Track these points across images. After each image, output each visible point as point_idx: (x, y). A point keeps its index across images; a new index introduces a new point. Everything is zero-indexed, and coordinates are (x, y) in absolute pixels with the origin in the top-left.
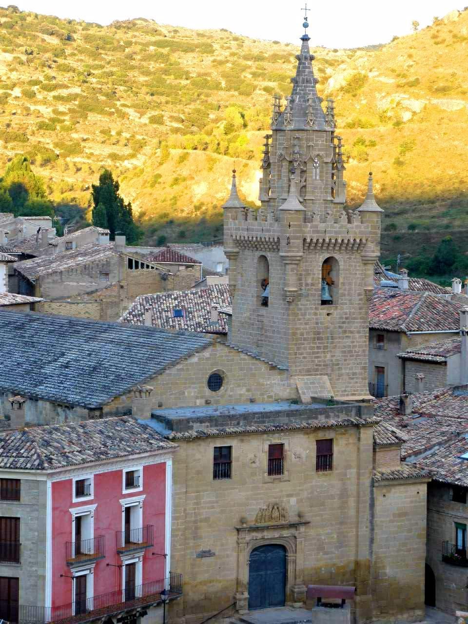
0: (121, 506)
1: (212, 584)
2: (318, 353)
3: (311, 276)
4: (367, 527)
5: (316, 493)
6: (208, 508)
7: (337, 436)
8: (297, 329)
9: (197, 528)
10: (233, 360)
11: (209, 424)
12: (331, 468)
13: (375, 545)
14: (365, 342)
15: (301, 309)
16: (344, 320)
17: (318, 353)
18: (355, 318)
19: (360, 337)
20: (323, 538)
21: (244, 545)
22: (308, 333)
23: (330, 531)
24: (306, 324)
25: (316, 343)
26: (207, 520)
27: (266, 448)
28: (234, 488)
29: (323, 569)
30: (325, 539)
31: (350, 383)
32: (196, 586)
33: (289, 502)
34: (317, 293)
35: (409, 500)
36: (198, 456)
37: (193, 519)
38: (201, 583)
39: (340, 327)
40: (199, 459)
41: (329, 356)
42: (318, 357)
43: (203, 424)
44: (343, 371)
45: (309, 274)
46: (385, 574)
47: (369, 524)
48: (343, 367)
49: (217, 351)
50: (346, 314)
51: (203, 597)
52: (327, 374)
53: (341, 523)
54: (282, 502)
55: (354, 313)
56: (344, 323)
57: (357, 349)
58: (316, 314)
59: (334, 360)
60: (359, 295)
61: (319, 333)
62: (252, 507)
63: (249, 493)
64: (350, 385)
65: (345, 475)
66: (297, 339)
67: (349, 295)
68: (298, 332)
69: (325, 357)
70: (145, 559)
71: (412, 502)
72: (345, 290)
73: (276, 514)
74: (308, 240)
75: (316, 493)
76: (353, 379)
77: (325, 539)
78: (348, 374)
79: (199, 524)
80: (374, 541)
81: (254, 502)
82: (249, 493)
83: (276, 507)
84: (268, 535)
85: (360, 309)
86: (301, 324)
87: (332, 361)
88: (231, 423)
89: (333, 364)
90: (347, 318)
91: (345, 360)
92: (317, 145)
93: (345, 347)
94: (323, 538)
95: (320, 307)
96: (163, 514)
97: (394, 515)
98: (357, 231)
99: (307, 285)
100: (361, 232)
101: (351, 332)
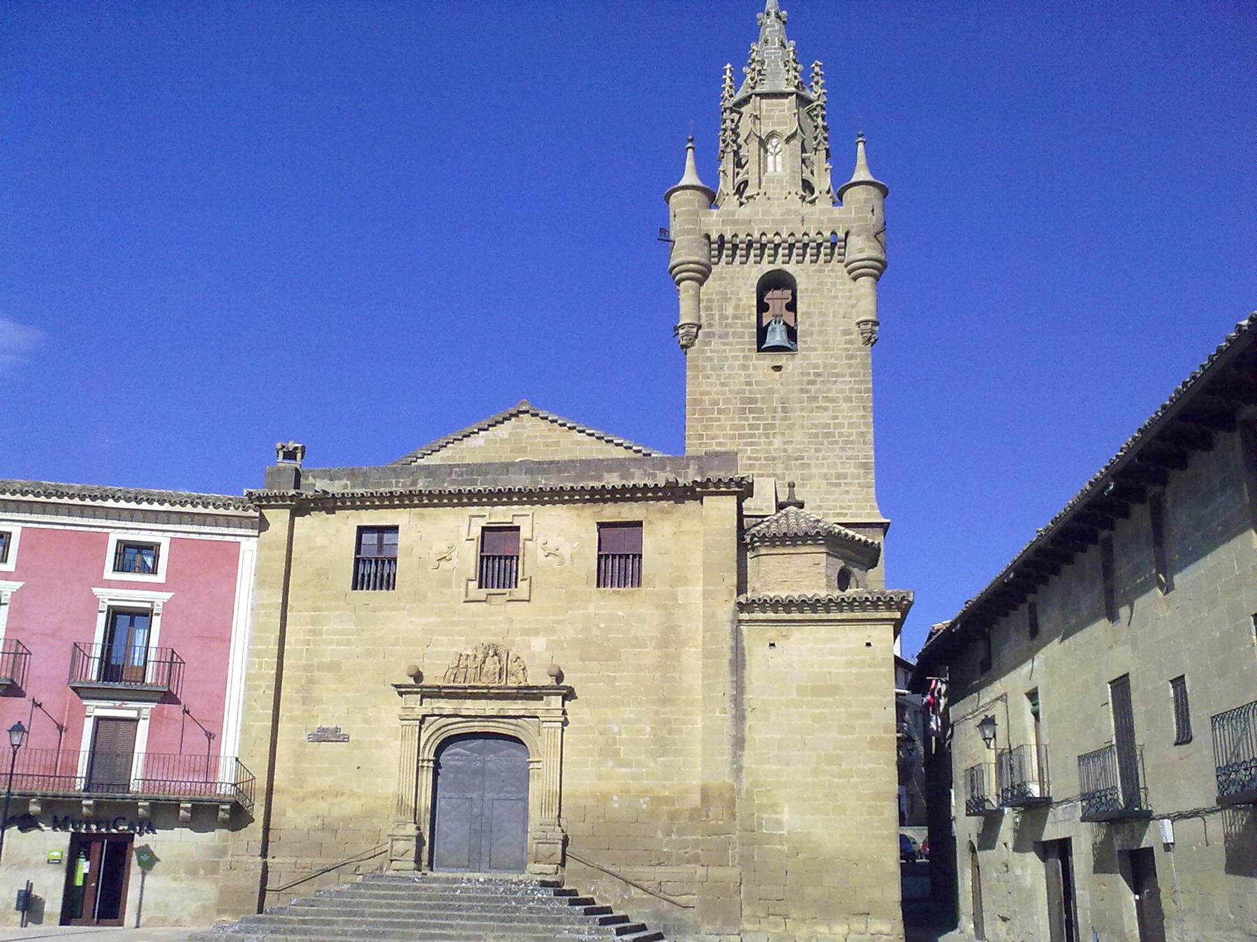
0: (95, 601)
1: (339, 799)
2: (752, 436)
3: (733, 303)
4: (724, 711)
5: (595, 631)
6: (338, 644)
7: (651, 517)
8: (702, 393)
9: (311, 681)
10: (558, 443)
11: (348, 483)
12: (637, 581)
13: (748, 758)
14: (864, 417)
15: (710, 359)
16: (812, 378)
17: (752, 436)
18: (837, 375)
19: (852, 409)
20: (616, 729)
22: (726, 401)
23: (632, 716)
24: (722, 384)
25: (747, 419)
26: (333, 667)
27: (477, 532)
28: (398, 609)
29: (615, 798)
30: (620, 733)
31: (833, 493)
32: (304, 799)
33: (529, 646)
34: (747, 331)
35: (844, 658)
36: (320, 541)
37: (304, 662)
38: (315, 794)
39: (802, 391)
40: (324, 547)
41: (777, 442)
42: (752, 444)
43: (336, 482)
44: (814, 470)
45: (727, 300)
46: (779, 823)
47: (728, 705)
48: (812, 462)
49: (525, 427)
50: (816, 366)
51: (318, 823)
52: (774, 475)
53: (664, 701)
54: (512, 643)
55: (835, 366)
56: (811, 383)
57: (845, 430)
58: (745, 367)
59: (789, 450)
60: (846, 332)
61: (752, 401)
63: (433, 620)
64: (830, 497)
65: (674, 597)
66: (703, 411)
67: (821, 332)
68: (706, 398)
69: (770, 443)
70: (155, 719)
71: (850, 664)
72: (812, 325)
73: (491, 665)
74: (714, 237)
75: (595, 631)
76: (838, 485)
77: (620, 733)
78: (825, 477)
79: (316, 673)
80: (746, 745)
81: (444, 639)
82: (433, 620)
84: (470, 707)
85: (851, 357)
86: (712, 384)
87: (785, 451)
88: (397, 482)
89: (789, 458)
90: (818, 375)
91: (817, 450)
92: (771, 117)
93: (815, 426)
94: (616, 729)
95: (754, 354)
96: (226, 640)
97: (801, 691)
98: (824, 218)
99: (723, 317)
100: (831, 220)
101: (831, 400)
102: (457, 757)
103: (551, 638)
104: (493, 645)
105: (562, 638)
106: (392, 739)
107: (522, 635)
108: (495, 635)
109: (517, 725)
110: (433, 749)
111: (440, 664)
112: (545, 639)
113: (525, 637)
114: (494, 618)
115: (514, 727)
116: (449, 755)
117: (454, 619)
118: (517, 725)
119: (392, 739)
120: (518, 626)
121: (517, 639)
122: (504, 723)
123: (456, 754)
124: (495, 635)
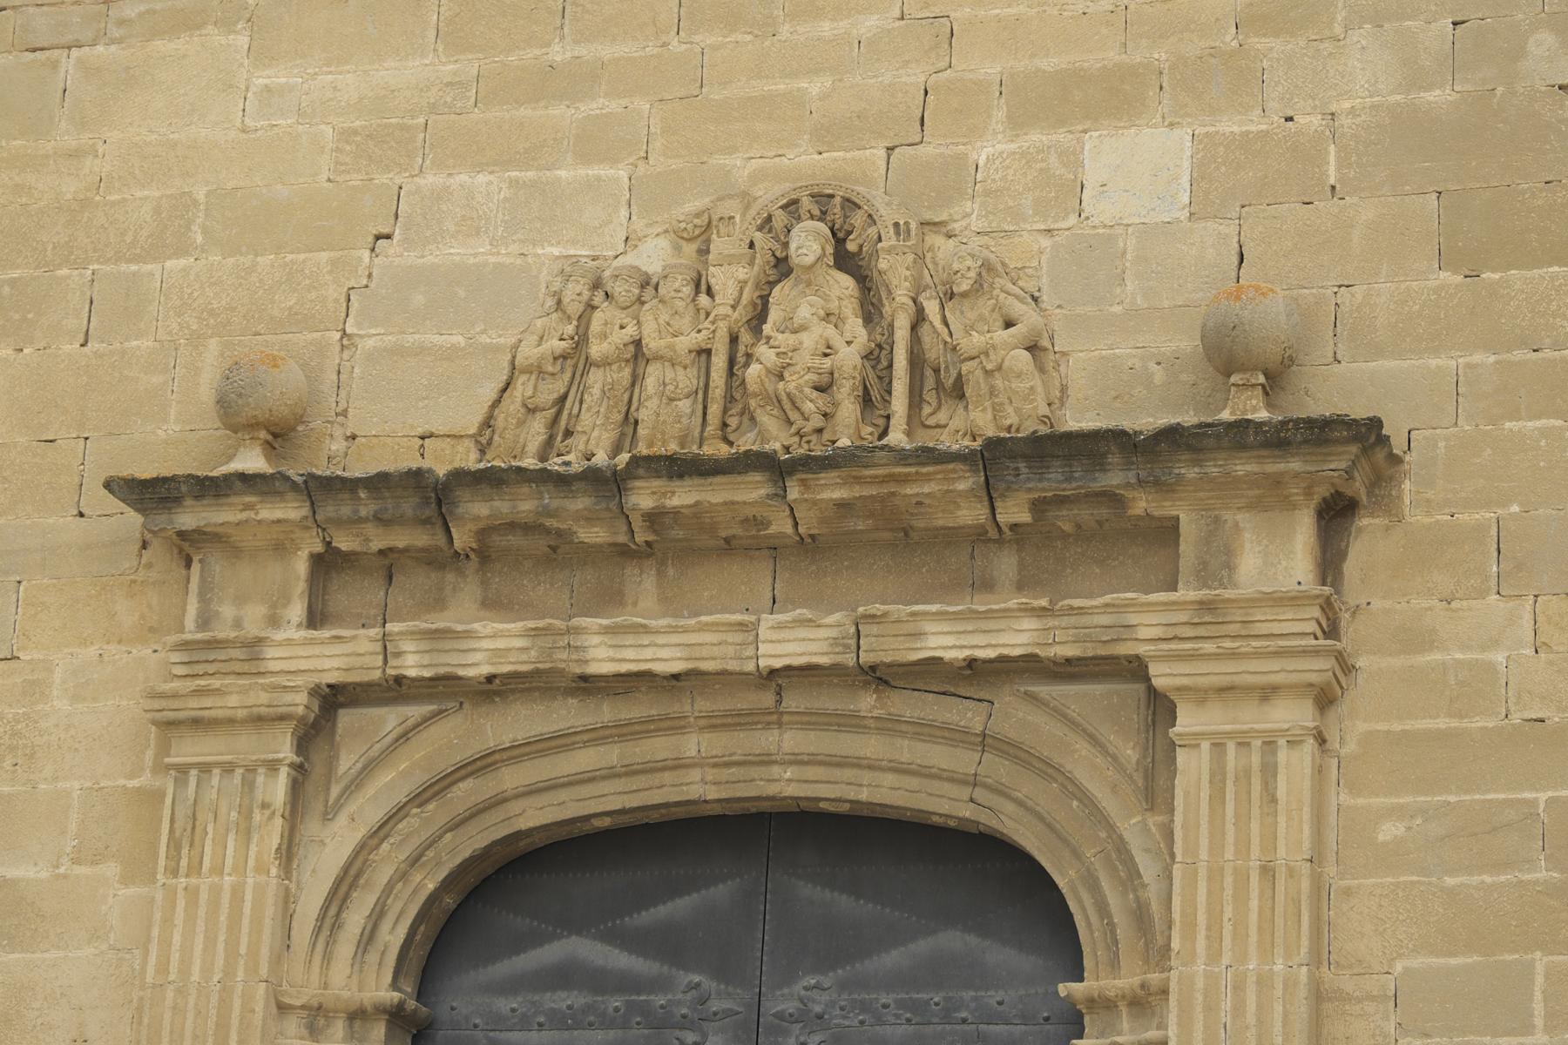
21: (247, 746)
62: (457, 252)
83: (808, 242)
102: (562, 1000)
103: (1230, 126)
104: (822, 199)
105: (1309, 122)
106: (111, 869)
107: (1018, 123)
108: (827, 135)
109: (984, 741)
110: (393, 936)
111: (451, 353)
112: (1183, 135)
113: (1036, 138)
114: (826, 28)
115: (964, 760)
116: (511, 986)
117: (558, 53)
118: (984, 741)
119: (111, 869)
120: (991, 70)
121: (982, 154)
122: (889, 726)
123: (563, 976)
124: (827, 135)
